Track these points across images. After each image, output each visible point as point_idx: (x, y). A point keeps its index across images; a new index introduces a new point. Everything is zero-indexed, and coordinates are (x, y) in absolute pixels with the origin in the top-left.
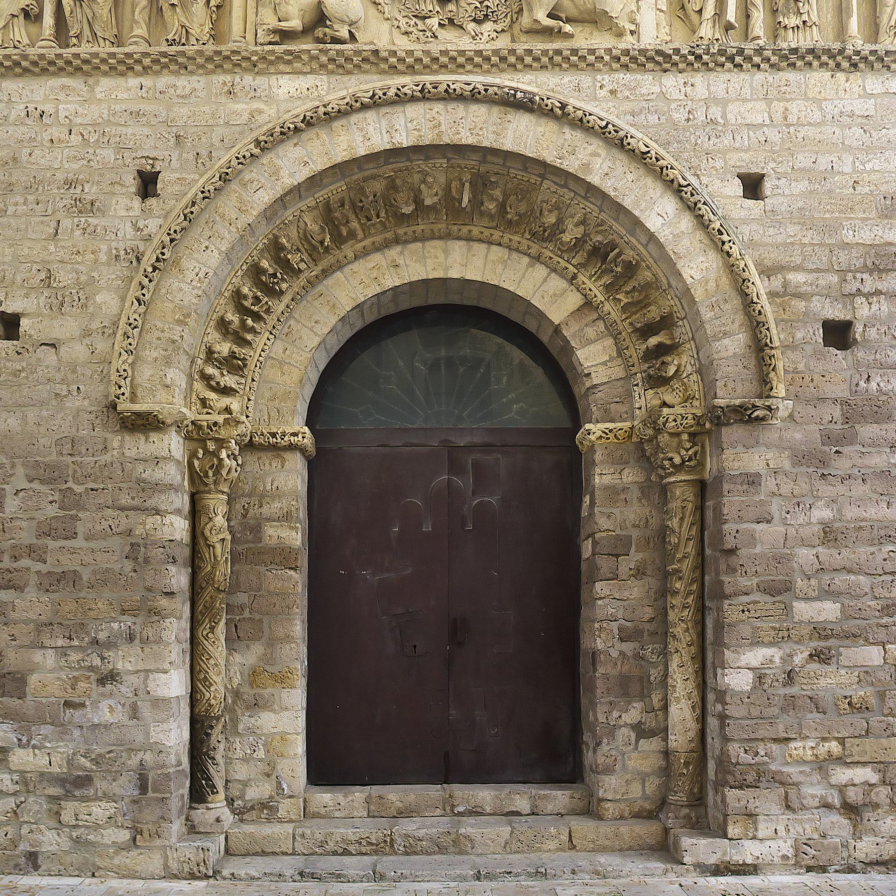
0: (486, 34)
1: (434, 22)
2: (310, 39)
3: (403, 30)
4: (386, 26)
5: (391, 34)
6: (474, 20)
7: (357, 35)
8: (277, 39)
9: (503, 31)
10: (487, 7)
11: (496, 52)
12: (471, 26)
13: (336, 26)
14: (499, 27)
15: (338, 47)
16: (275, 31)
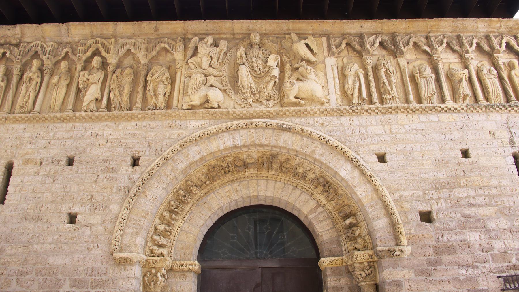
0: (271, 105)
1: (251, 100)
2: (203, 107)
3: (238, 104)
4: (232, 102)
5: (234, 104)
6: (266, 100)
7: (221, 105)
8: (190, 108)
9: (277, 103)
10: (271, 95)
11: (275, 111)
12: (265, 102)
13: (213, 103)
14: (276, 102)
15: (213, 110)
16: (189, 105)
